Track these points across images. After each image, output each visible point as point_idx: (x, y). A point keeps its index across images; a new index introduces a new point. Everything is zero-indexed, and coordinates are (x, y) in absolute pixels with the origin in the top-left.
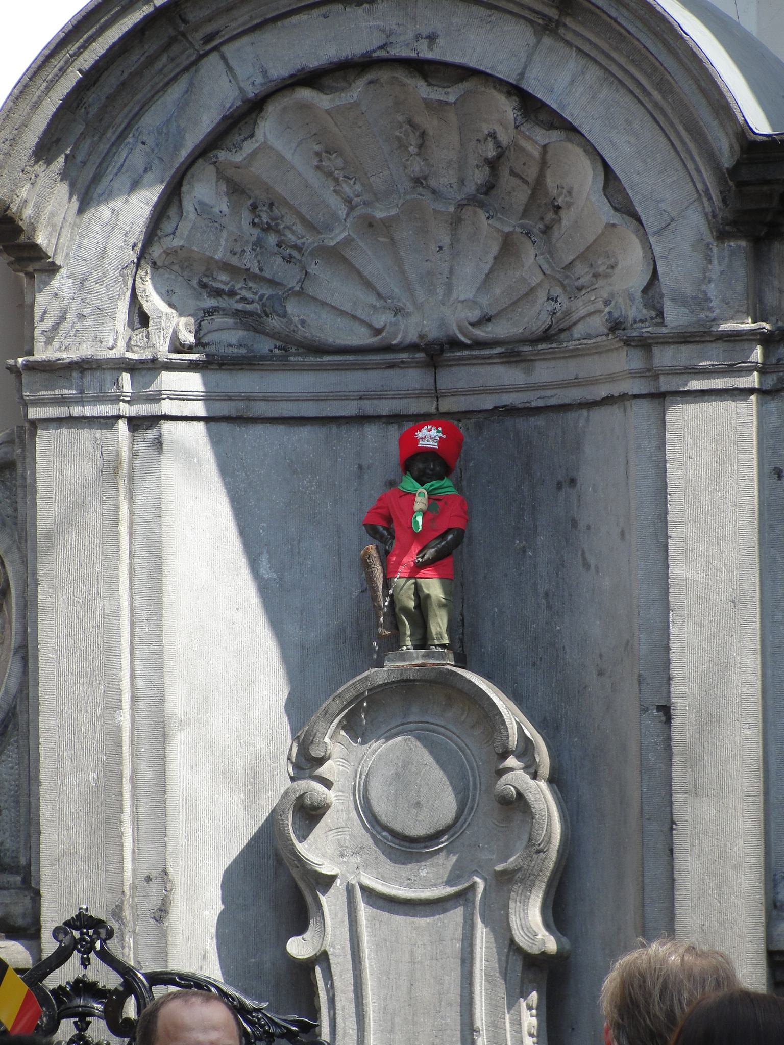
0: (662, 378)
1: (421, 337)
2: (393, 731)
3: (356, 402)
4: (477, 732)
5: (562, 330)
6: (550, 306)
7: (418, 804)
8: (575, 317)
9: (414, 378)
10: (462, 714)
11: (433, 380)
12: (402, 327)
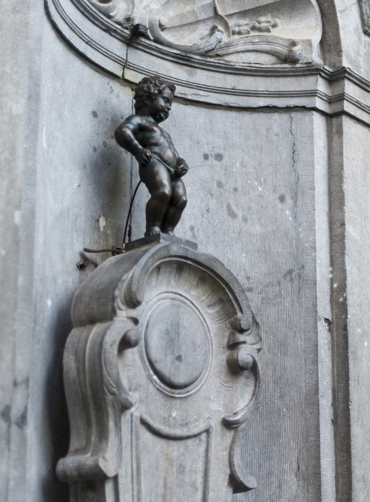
0: (345, 101)
1: (128, 19)
2: (163, 295)
3: (84, 43)
4: (210, 311)
5: (218, 55)
6: (217, 35)
7: (179, 358)
8: (232, 50)
9: (117, 47)
10: (204, 295)
11: (126, 54)
12: (118, 6)
